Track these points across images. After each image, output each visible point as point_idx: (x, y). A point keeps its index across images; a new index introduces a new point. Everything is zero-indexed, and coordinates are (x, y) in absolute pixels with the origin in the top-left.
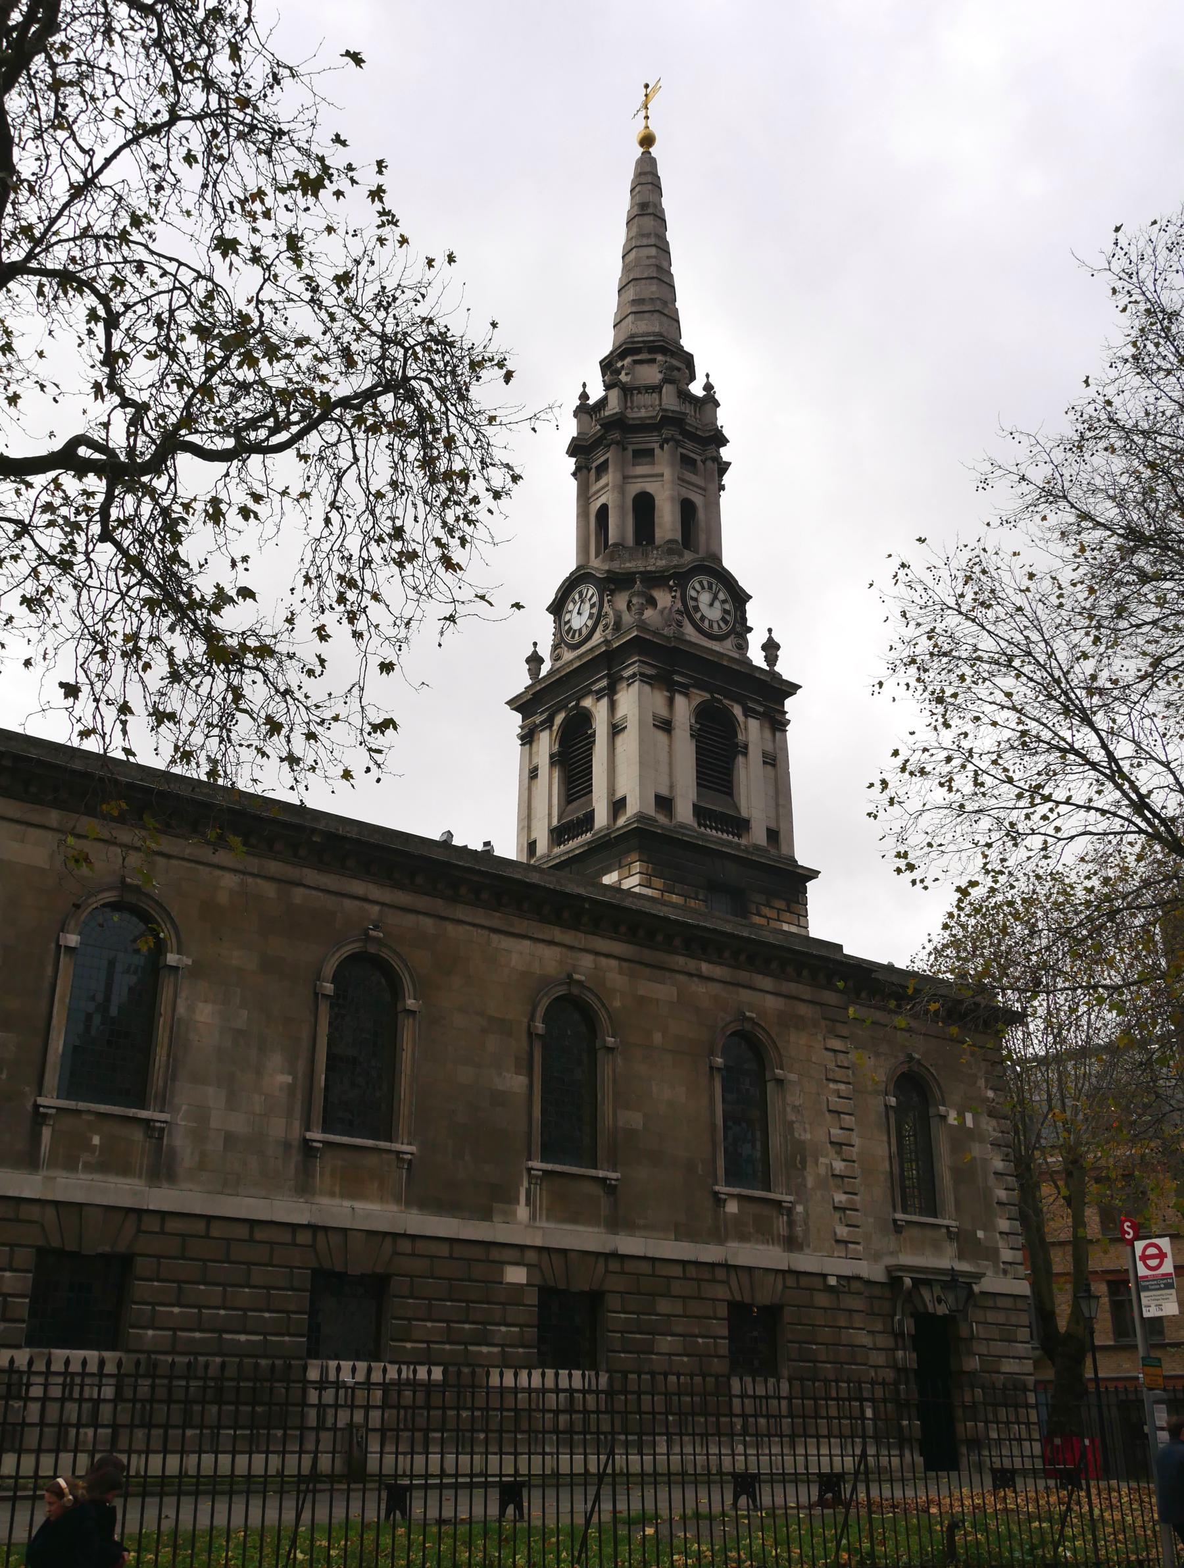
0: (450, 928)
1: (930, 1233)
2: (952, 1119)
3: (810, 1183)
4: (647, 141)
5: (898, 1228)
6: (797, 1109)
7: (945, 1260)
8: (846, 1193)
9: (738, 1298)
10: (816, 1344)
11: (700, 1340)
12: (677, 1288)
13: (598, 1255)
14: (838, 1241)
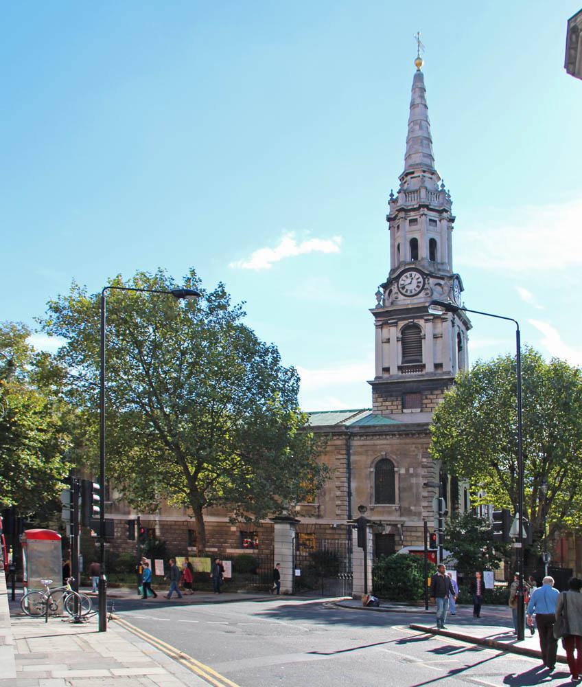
2: (403, 471)
7: (394, 518)
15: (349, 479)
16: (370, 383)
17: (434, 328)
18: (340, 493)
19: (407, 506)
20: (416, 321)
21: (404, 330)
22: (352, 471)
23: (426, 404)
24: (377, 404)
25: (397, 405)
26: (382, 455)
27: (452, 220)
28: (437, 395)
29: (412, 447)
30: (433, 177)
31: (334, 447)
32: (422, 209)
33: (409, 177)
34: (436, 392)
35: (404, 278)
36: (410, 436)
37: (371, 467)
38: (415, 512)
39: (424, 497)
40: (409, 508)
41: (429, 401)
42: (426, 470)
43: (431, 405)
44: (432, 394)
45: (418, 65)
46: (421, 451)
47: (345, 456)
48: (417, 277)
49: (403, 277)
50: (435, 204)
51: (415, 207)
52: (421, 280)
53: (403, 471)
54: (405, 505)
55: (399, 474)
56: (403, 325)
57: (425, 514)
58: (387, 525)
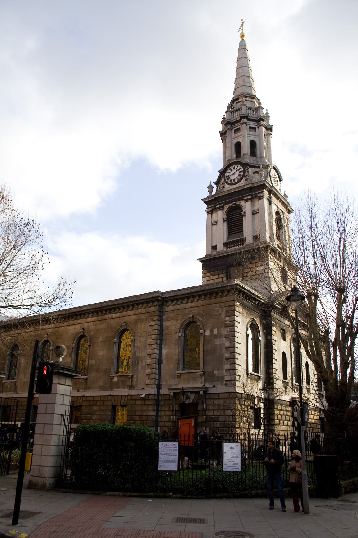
0: (60, 329)
1: (192, 375)
2: (208, 333)
4: (242, 36)
5: (179, 376)
6: (137, 347)
7: (198, 384)
8: (151, 369)
10: (136, 415)
12: (98, 403)
13: (81, 396)
16: (201, 260)
17: (253, 206)
18: (150, 360)
19: (210, 370)
20: (238, 203)
21: (228, 213)
24: (206, 279)
25: (222, 278)
26: (190, 318)
27: (270, 129)
29: (216, 307)
31: (148, 314)
32: (243, 119)
33: (235, 102)
36: (214, 295)
38: (218, 377)
39: (227, 359)
40: (213, 372)
41: (249, 270)
42: (228, 329)
45: (242, 36)
46: (224, 309)
47: (159, 323)
48: (239, 168)
50: (254, 115)
51: (238, 119)
53: (208, 333)
54: (209, 369)
55: (204, 336)
56: (227, 208)
57: (227, 378)
58: (191, 392)
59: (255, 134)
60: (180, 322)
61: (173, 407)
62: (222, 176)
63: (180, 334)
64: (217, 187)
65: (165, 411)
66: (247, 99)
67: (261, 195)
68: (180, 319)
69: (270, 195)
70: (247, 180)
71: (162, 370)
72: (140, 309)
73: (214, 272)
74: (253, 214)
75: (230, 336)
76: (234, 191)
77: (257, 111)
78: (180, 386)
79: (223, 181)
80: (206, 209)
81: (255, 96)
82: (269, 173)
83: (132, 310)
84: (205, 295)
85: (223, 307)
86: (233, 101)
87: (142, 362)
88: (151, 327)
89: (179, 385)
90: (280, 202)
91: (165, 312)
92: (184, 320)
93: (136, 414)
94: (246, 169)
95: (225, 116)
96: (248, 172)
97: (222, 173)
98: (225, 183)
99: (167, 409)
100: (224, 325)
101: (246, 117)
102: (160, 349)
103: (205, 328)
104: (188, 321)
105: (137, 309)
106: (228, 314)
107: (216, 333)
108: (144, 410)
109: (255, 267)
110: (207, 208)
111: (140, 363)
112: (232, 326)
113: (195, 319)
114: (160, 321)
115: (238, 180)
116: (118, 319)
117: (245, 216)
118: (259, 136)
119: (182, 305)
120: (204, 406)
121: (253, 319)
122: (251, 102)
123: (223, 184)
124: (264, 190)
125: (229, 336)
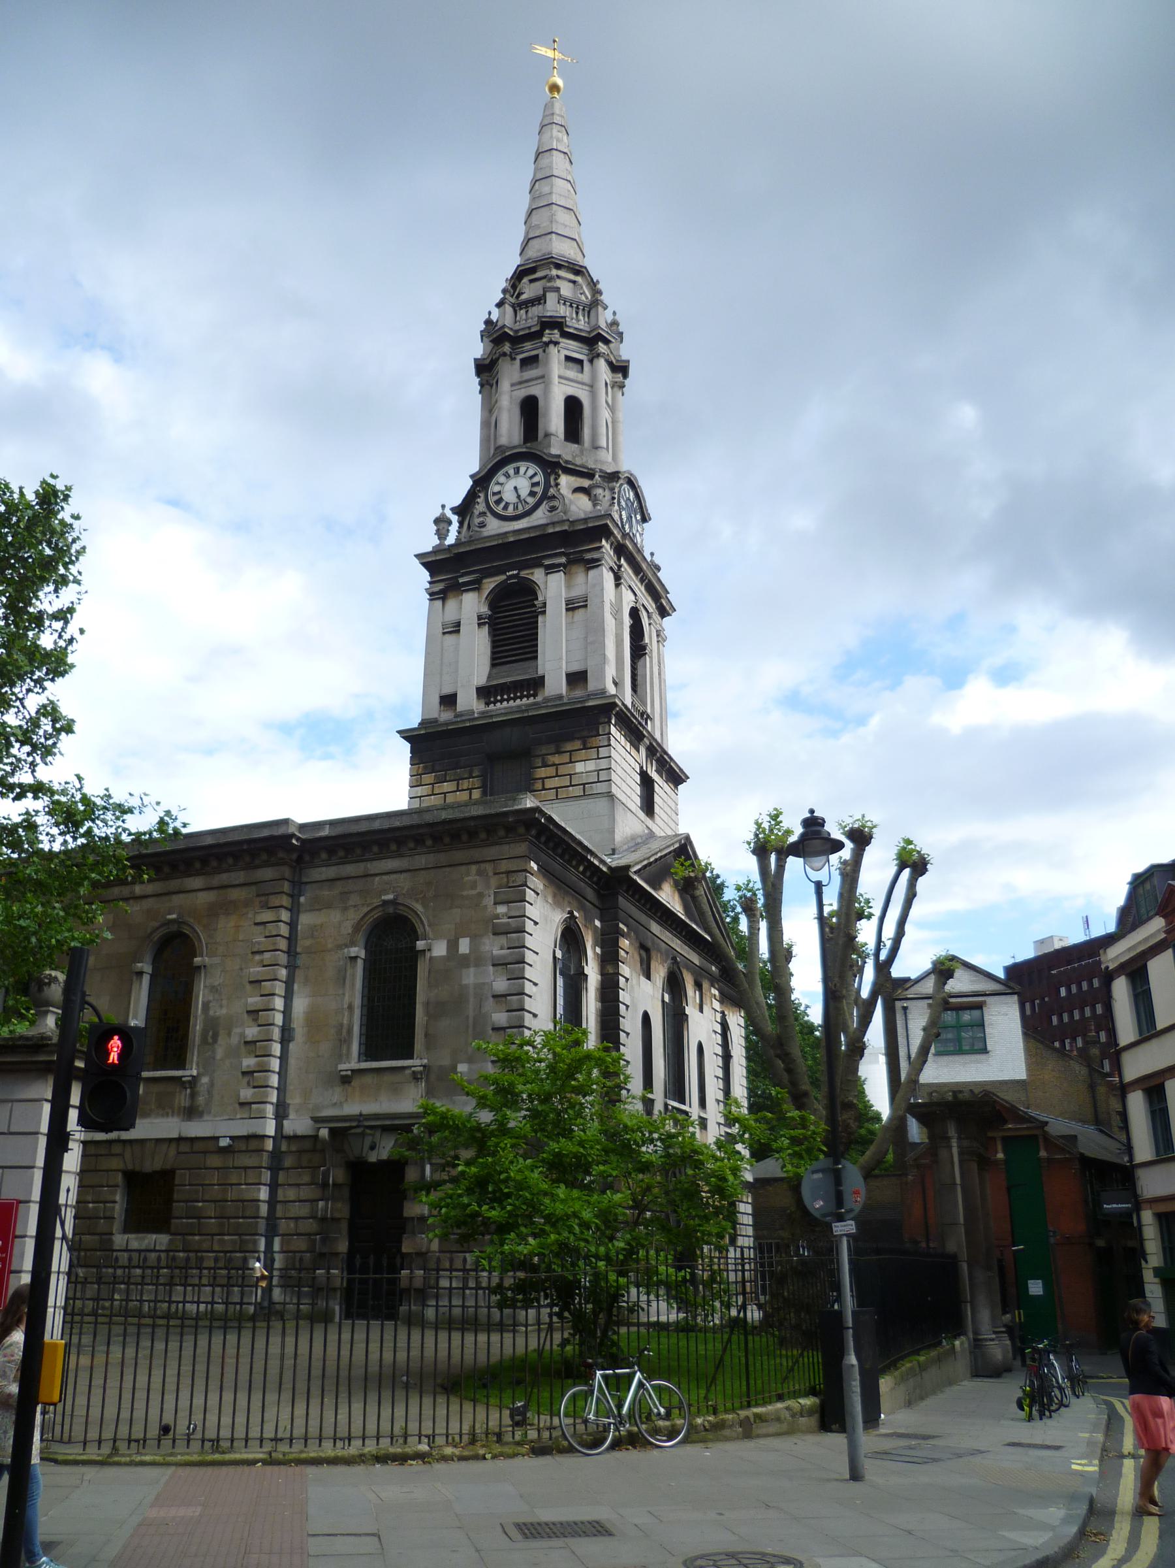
1: (388, 1078)
2: (440, 949)
3: (220, 1052)
5: (346, 1080)
6: (214, 989)
8: (257, 1056)
9: (130, 1167)
10: (203, 1201)
11: (91, 1205)
14: (242, 1104)
15: (289, 984)
16: (407, 735)
17: (569, 586)
19: (446, 1062)
20: (524, 573)
21: (496, 601)
22: (301, 960)
23: (543, 779)
24: (419, 791)
25: (470, 790)
26: (385, 903)
27: (620, 369)
28: (570, 752)
29: (468, 874)
30: (579, 279)
31: (254, 888)
32: (547, 331)
33: (525, 280)
34: (569, 746)
35: (502, 479)
37: (353, 944)
39: (496, 1029)
41: (551, 771)
42: (503, 940)
43: (556, 782)
44: (559, 752)
46: (494, 881)
48: (531, 472)
49: (500, 477)
50: (579, 324)
51: (533, 330)
52: (539, 478)
53: (440, 949)
55: (431, 958)
56: (492, 586)
58: (386, 1129)
59: (580, 379)
60: (353, 916)
61: (326, 1175)
62: (479, 491)
63: (354, 951)
64: (461, 523)
65: (298, 1185)
66: (561, 273)
67: (595, 555)
68: (355, 906)
69: (619, 559)
70: (553, 509)
71: (292, 1062)
72: (228, 871)
73: (446, 770)
74: (567, 610)
75: (510, 960)
76: (517, 538)
77: (589, 312)
78: (352, 1108)
79: (480, 507)
80: (428, 586)
81: (586, 268)
82: (616, 496)
83: (198, 873)
84: (437, 839)
85: (491, 874)
86: (520, 274)
87: (229, 1034)
88: (262, 927)
89: (345, 1106)
90: (642, 581)
91: (307, 883)
92: (365, 910)
93: (207, 1197)
94: (552, 478)
95: (494, 318)
96: (557, 485)
97: (481, 482)
98: (488, 514)
99: (306, 1179)
100: (491, 927)
101: (556, 324)
102: (288, 998)
103: (431, 935)
104: (376, 914)
105: (218, 871)
106: (501, 898)
107: (468, 952)
108: (232, 1185)
109: (571, 762)
110: (430, 583)
111: (220, 1038)
112: (515, 930)
113: (401, 908)
114: (290, 910)
115: (527, 507)
116: (150, 900)
117: (544, 612)
118: (592, 386)
119: (362, 865)
120: (423, 1171)
121: (571, 913)
122: (571, 285)
123: (483, 514)
124: (604, 542)
125: (506, 961)
